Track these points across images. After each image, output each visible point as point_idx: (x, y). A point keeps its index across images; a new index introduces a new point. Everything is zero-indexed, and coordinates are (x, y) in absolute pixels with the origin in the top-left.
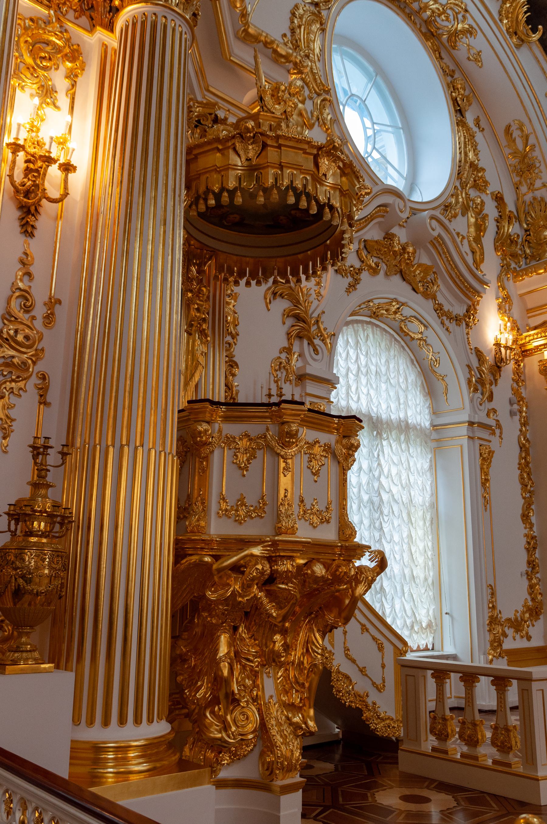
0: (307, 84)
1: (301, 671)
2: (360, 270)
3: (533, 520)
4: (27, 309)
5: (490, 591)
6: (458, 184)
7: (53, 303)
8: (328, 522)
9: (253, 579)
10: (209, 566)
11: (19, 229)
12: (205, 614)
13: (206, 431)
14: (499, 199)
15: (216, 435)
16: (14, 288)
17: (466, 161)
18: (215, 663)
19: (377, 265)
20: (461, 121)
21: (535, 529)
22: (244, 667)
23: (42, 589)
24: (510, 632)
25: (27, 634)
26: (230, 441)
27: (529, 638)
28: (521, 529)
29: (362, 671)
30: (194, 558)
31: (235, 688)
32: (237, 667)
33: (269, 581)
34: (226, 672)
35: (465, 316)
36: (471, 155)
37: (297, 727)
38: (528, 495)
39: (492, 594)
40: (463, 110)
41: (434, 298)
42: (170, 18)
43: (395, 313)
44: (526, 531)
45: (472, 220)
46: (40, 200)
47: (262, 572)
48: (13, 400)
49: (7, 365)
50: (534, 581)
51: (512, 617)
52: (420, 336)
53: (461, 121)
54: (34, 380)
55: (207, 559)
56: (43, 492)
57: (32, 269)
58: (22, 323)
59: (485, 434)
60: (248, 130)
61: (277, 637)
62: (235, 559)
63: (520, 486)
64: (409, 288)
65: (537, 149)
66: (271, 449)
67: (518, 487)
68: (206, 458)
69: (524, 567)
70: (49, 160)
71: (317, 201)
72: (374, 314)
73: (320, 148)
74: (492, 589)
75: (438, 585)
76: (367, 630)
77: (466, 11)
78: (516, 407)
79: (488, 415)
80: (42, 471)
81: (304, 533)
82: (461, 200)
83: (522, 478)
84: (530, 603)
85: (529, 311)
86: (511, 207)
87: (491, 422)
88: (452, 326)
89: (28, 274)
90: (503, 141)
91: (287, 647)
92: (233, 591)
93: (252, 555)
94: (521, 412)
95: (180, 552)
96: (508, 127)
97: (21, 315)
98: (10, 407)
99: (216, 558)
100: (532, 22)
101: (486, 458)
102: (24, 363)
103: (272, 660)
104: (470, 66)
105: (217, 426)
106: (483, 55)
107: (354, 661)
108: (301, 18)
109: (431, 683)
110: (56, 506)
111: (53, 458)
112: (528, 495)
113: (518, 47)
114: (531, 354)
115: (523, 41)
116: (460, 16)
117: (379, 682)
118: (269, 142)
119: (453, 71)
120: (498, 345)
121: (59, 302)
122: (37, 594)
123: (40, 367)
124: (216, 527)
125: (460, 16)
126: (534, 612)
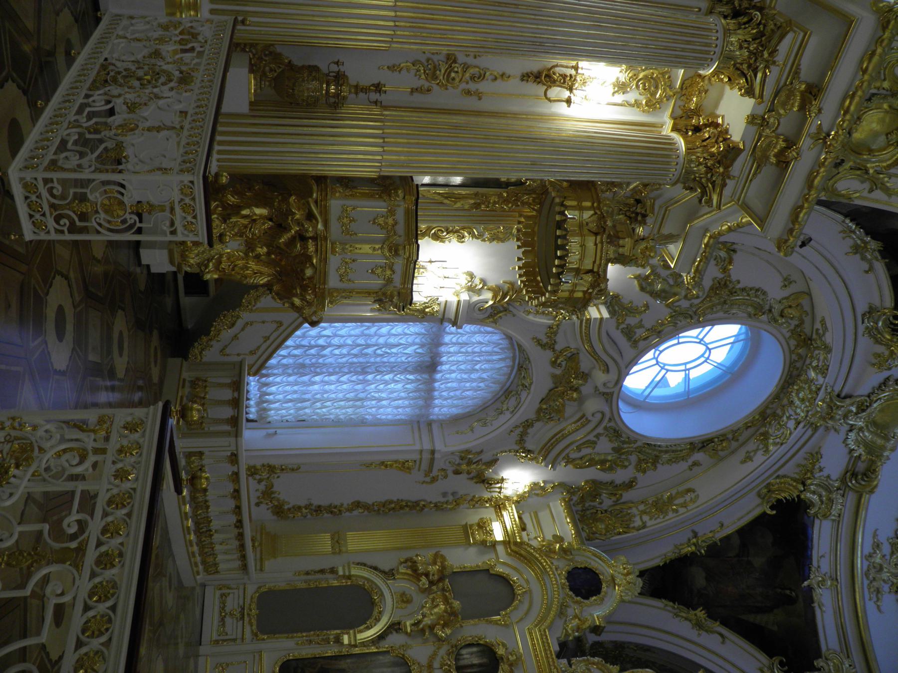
0: (702, 302)
1: (242, 269)
2: (554, 350)
3: (355, 513)
4: (473, 78)
5: (295, 467)
6: (639, 444)
7: (479, 96)
8: (341, 280)
9: (303, 225)
10: (311, 196)
11: (525, 72)
12: (280, 198)
13: (398, 196)
14: (630, 485)
15: (396, 203)
16: (485, 70)
17: (661, 451)
18: (248, 206)
19: (560, 365)
20: (695, 448)
21: (348, 513)
22: (246, 227)
23: (296, 92)
24: (262, 487)
25: (270, 85)
26: (392, 212)
27: (257, 505)
28: (347, 501)
29: (235, 337)
30: (315, 188)
31: (234, 220)
32: (245, 222)
33: (302, 237)
34: (245, 212)
35: (524, 448)
36: (666, 456)
37: (207, 266)
38: (376, 508)
39: (293, 470)
40: (704, 449)
41: (538, 420)
42: (677, 167)
43: (523, 385)
44: (345, 505)
45: (610, 458)
46: (544, 84)
47: (307, 231)
48: (413, 72)
49: (435, 67)
50: (304, 511)
51: (274, 489)
52: (505, 408)
53: (695, 448)
54: (427, 85)
55: (315, 195)
56: (353, 90)
57: (499, 81)
58: (463, 75)
59: (425, 465)
60: (605, 222)
61: (265, 249)
62: (315, 212)
63: (383, 501)
64: (543, 393)
65: (675, 515)
66: (388, 238)
67: (383, 499)
68: (380, 197)
69: (316, 502)
70: (571, 89)
71: (562, 273)
72: (521, 366)
73: (598, 273)
74: (297, 469)
75: (301, 423)
76: (265, 341)
77: (782, 444)
78: (451, 498)
79: (443, 470)
80: (365, 90)
81: (334, 261)
82: (625, 446)
83: (391, 502)
84: (286, 507)
85: (536, 514)
86: (627, 496)
87: (435, 473)
88: (515, 435)
89: (496, 79)
90: (682, 488)
91: (258, 257)
92: (295, 213)
93: (318, 223)
94: (447, 503)
95: (321, 180)
96: (693, 491)
97: (467, 75)
98: (408, 70)
99: (316, 202)
100: (778, 505)
101: (404, 466)
102: (437, 78)
103: (250, 246)
104: (741, 454)
105: (402, 203)
106: (750, 463)
107: (243, 330)
108: (756, 296)
109: (228, 381)
110: (344, 98)
111: (374, 96)
112: (376, 508)
113: (759, 495)
114: (496, 512)
115: (763, 498)
116: (778, 440)
117: (227, 351)
118: (599, 238)
119: (737, 440)
120: (503, 480)
121: (480, 99)
122: (293, 89)
123: (435, 87)
124: (335, 204)
125: (778, 440)
126: (279, 511)
